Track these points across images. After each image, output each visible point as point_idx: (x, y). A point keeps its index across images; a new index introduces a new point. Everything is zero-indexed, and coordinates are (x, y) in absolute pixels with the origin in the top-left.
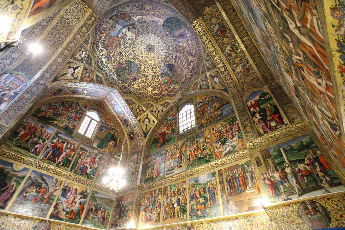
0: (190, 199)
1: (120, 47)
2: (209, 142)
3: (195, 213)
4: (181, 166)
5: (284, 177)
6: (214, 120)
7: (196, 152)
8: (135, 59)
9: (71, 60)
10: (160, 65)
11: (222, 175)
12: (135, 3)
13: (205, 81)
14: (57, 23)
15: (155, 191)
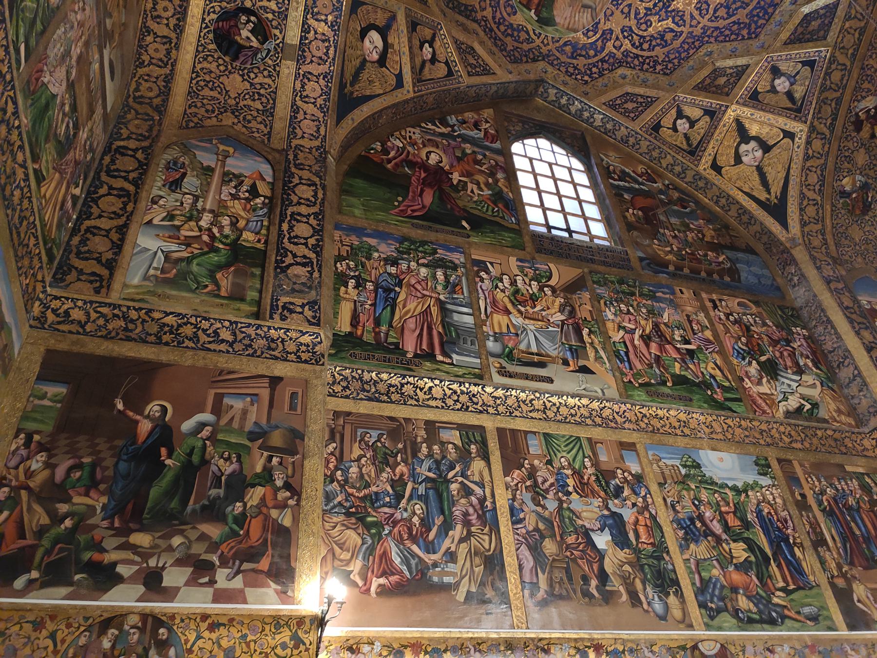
0: (681, 533)
2: (708, 341)
3: (722, 599)
4: (584, 370)
6: (710, 273)
7: (653, 346)
11: (797, 480)
15: (431, 426)
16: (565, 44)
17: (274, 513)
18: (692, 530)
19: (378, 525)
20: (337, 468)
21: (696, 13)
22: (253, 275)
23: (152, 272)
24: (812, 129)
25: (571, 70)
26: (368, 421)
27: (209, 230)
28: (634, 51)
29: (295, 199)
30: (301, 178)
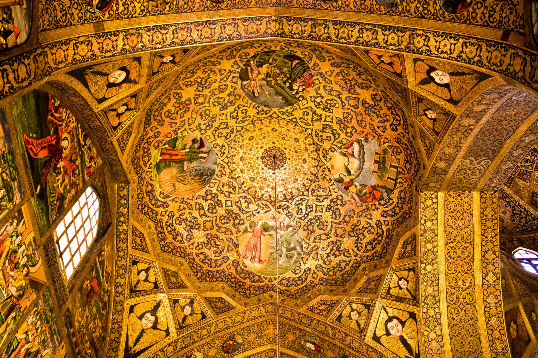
1: (339, 121)
8: (285, 117)
9: (449, 107)
10: (226, 152)
12: (372, 236)
13: (146, 280)
14: (501, 148)
16: (151, 185)
21: (196, 244)
25: (140, 196)
28: (164, 224)
30: (29, 64)
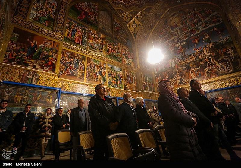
4: (102, 52)
5: (147, 85)
17: (53, 61)
18: (110, 75)
19: (68, 66)
20: (62, 57)
22: (52, 23)
23: (34, 18)
24: (143, 25)
26: (68, 52)
27: (45, 12)
29: (61, 11)
